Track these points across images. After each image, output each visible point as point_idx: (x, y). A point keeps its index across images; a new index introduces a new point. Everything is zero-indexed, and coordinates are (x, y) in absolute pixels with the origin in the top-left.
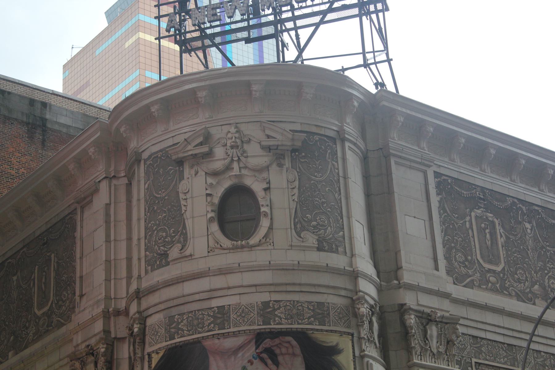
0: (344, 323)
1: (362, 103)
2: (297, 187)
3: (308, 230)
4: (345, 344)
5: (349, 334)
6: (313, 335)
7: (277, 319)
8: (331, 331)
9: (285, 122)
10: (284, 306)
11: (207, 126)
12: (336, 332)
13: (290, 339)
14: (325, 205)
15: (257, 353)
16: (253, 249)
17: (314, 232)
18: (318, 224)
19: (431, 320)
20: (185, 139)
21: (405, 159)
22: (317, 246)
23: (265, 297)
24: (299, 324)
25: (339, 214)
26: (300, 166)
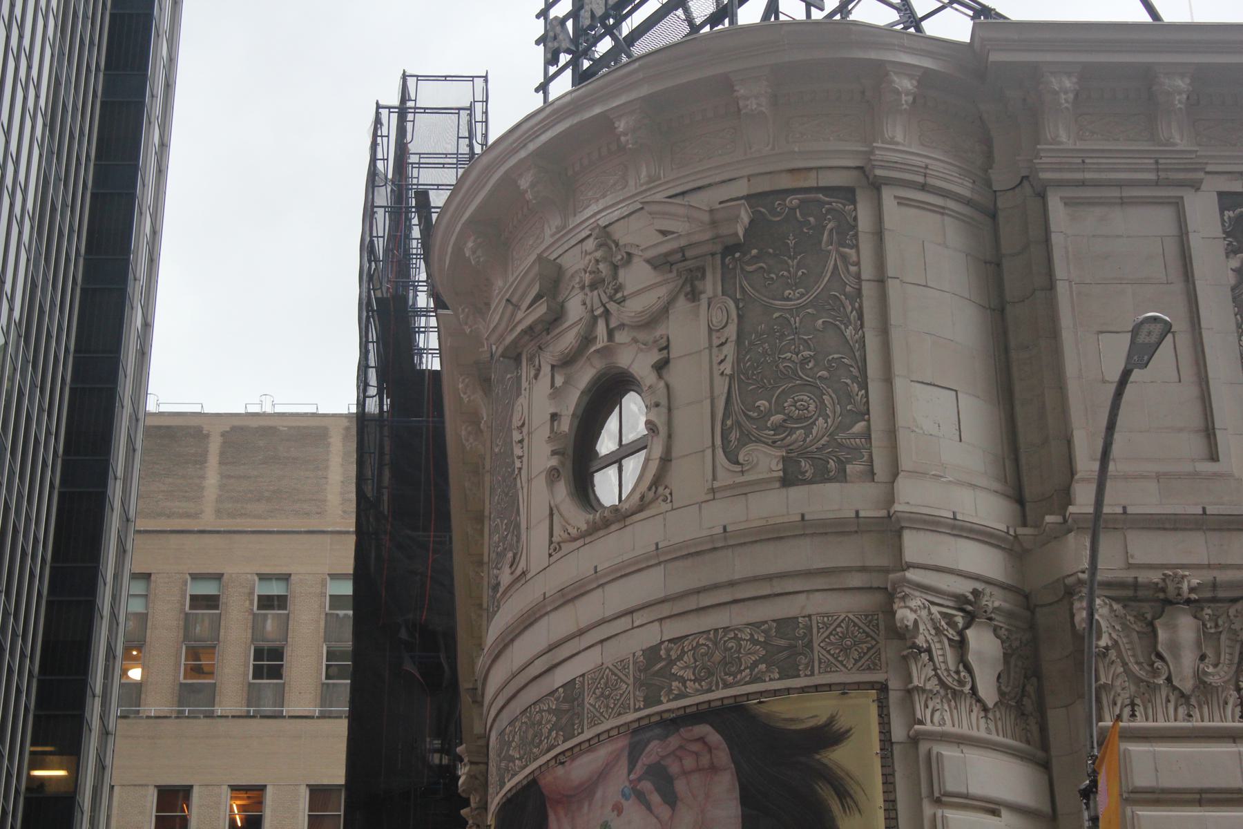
0: (856, 661)
1: (925, 78)
2: (734, 337)
3: (758, 441)
4: (860, 715)
5: (872, 685)
6: (764, 709)
7: (675, 684)
8: (817, 688)
9: (710, 185)
10: (693, 648)
11: (538, 251)
12: (830, 687)
13: (704, 729)
14: (811, 365)
15: (631, 782)
16: (628, 521)
17: (774, 442)
18: (789, 418)
19: (1168, 602)
21: (1097, 184)
22: (781, 474)
23: (650, 636)
24: (727, 686)
25: (854, 379)
26: (745, 283)
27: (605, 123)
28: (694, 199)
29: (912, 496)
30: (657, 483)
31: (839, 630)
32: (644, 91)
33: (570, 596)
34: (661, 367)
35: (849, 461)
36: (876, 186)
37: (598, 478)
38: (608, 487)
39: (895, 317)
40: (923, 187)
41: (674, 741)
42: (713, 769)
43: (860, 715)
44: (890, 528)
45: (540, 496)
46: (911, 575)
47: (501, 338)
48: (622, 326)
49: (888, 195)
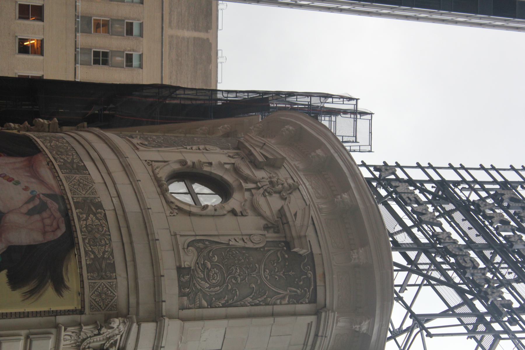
0: (95, 300)
1: (367, 337)
2: (247, 246)
3: (198, 256)
4: (69, 301)
5: (83, 307)
6: (72, 256)
7: (85, 216)
8: (82, 281)
9: (317, 236)
10: (101, 225)
11: (287, 158)
12: (83, 287)
13: (63, 229)
14: (234, 281)
15: (39, 195)
16: (161, 196)
17: (198, 263)
18: (209, 271)
20: (265, 144)
22: (183, 266)
23: (107, 205)
24: (84, 240)
25: (227, 301)
26: (272, 251)
27: (347, 188)
28: (311, 227)
29: (172, 327)
30: (180, 210)
31: (109, 292)
32: (361, 206)
33: (127, 169)
34: (233, 212)
35: (189, 298)
36: (317, 313)
37: (182, 184)
38: (177, 188)
39: (255, 321)
40: (316, 335)
41: (58, 215)
42: (44, 233)
43: (69, 301)
44: (157, 317)
45: (173, 157)
46: (135, 326)
47: (247, 141)
48: (252, 195)
49: (312, 319)
